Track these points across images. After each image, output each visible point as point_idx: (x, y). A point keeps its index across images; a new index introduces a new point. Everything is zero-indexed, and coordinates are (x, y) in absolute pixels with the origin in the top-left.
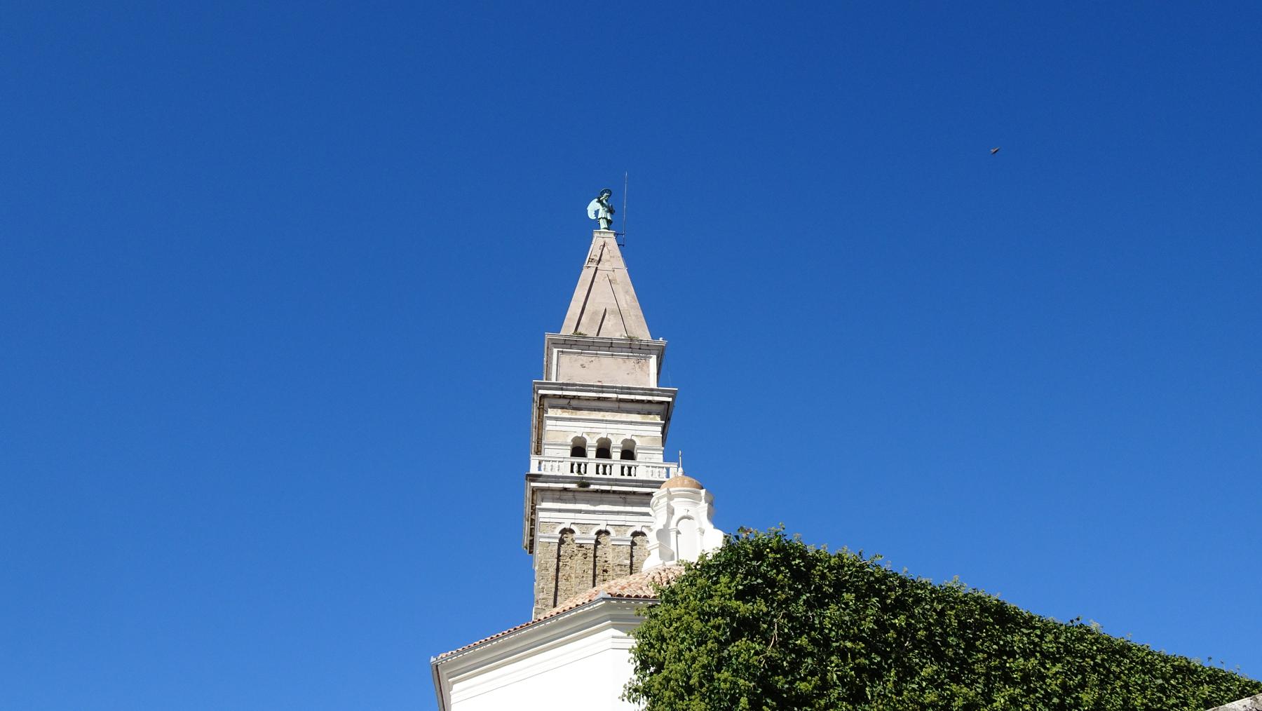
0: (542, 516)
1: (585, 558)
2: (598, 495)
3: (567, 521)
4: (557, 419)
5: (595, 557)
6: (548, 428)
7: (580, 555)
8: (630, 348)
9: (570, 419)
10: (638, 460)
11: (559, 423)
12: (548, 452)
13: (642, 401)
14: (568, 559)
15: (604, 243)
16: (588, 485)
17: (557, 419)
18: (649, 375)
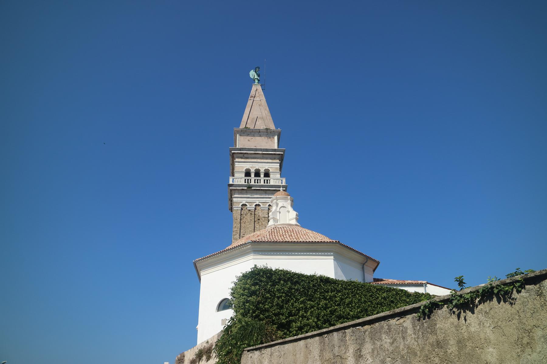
0: (235, 200)
1: (251, 215)
2: (255, 191)
3: (244, 201)
4: (239, 162)
5: (255, 214)
6: (236, 166)
7: (249, 214)
8: (267, 133)
9: (244, 162)
10: (271, 177)
11: (240, 163)
12: (236, 175)
13: (272, 154)
14: (244, 216)
15: (257, 89)
16: (251, 187)
17: (239, 162)
18: (274, 143)
